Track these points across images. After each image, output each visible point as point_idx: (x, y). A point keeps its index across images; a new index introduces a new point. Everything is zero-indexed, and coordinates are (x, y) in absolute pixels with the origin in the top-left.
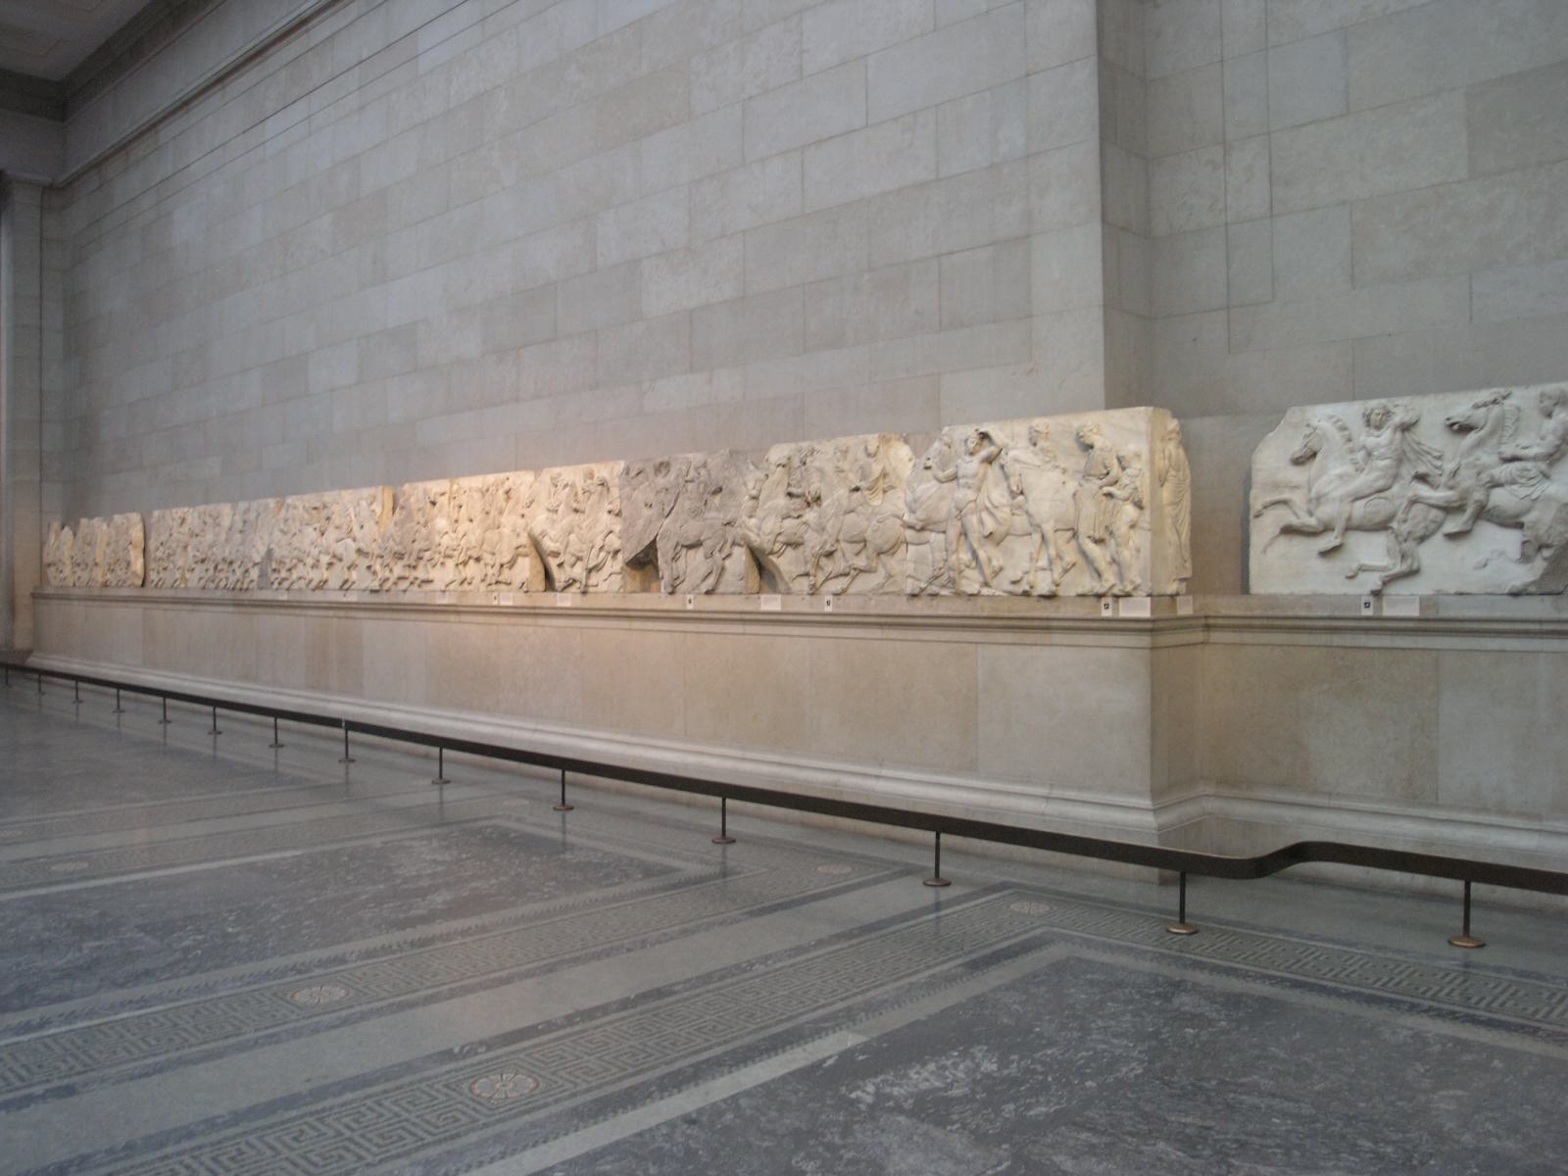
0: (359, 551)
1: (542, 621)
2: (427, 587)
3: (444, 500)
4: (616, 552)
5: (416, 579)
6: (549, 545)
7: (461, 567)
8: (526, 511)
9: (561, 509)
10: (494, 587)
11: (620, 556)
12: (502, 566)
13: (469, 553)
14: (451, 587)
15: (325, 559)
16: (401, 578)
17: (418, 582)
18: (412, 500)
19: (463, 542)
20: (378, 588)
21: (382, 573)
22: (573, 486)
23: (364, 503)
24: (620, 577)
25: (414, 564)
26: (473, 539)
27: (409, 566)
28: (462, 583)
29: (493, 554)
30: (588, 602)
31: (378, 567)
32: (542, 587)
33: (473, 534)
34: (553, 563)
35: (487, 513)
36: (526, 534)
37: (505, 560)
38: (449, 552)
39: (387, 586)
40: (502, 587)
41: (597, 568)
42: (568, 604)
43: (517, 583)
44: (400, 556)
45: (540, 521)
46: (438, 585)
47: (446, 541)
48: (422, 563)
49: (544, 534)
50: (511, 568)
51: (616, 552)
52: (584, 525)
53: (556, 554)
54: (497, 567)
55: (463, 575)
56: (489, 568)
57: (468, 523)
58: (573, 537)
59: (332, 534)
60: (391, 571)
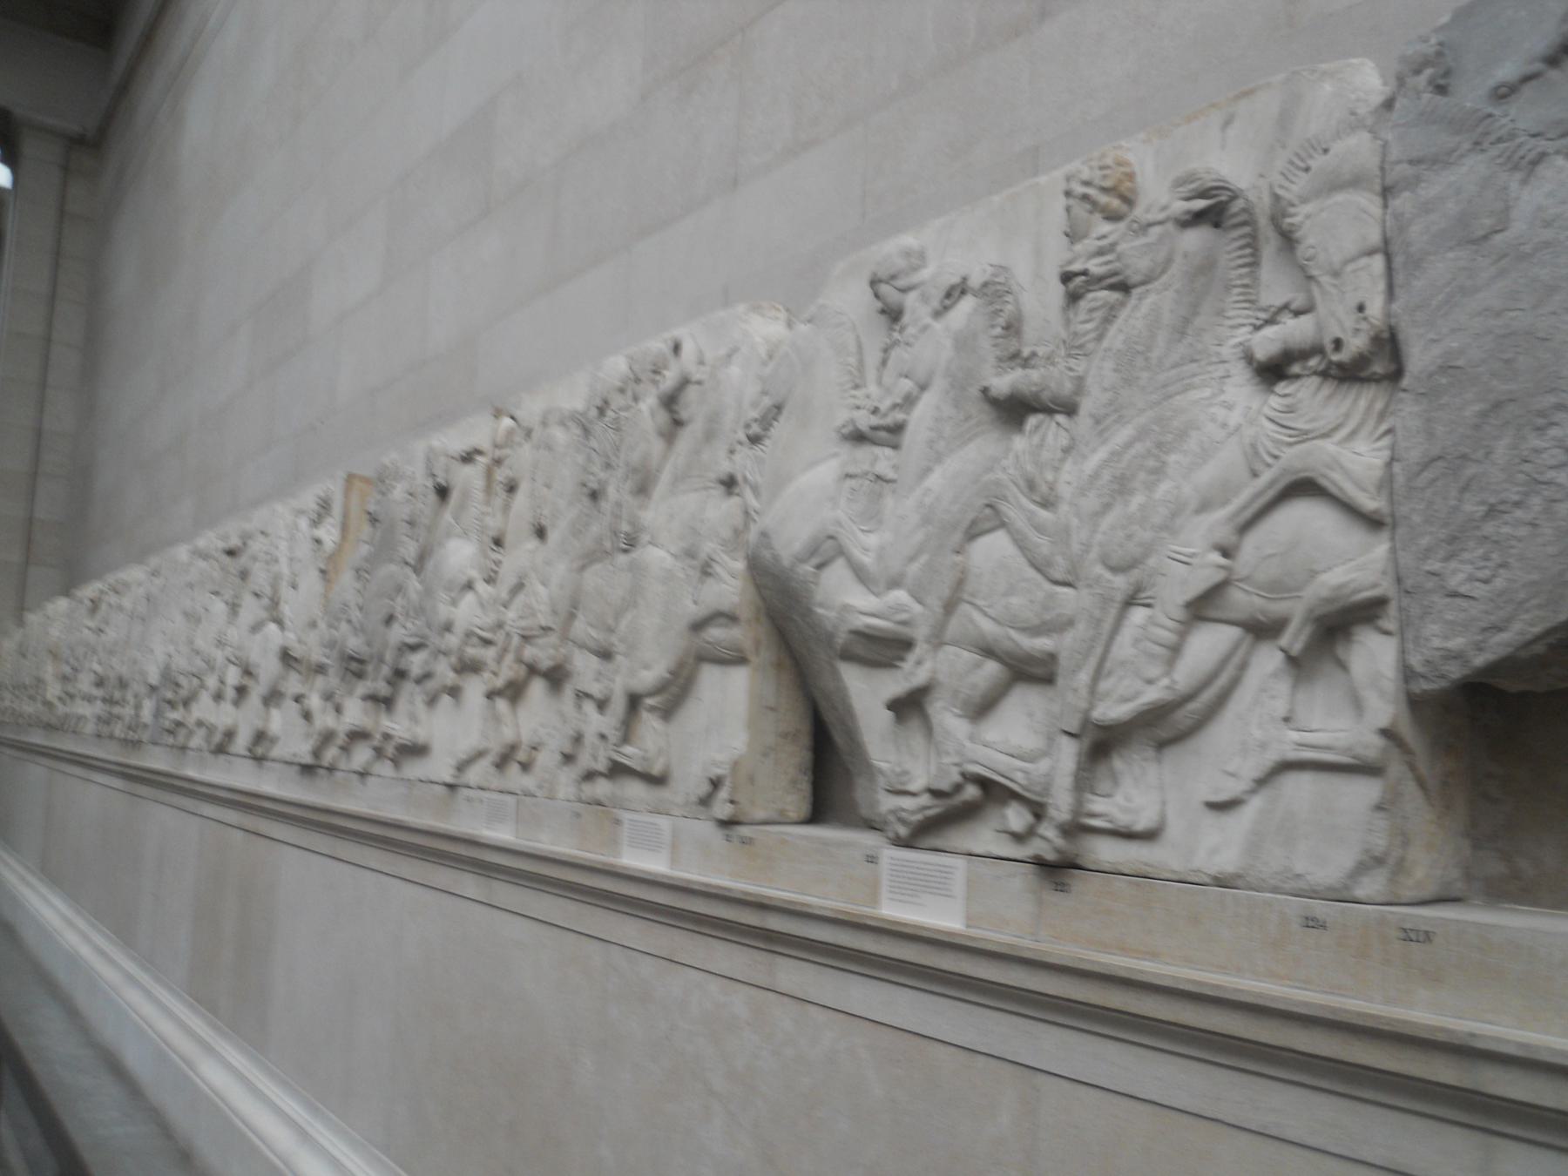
0: (286, 657)
1: (792, 974)
2: (415, 769)
3: (469, 478)
4: (1338, 625)
5: (387, 737)
6: (847, 601)
7: (502, 705)
8: (743, 463)
9: (920, 419)
10: (602, 788)
11: (1374, 656)
12: (634, 702)
13: (529, 652)
14: (474, 775)
15: (233, 676)
16: (358, 735)
17: (390, 750)
18: (398, 492)
19: (510, 615)
20: (308, 760)
21: (325, 720)
22: (994, 292)
23: (303, 523)
24: (1365, 791)
25: (383, 689)
26: (541, 599)
27: (373, 698)
28: (502, 762)
29: (605, 655)
30: (1074, 931)
31: (315, 702)
32: (797, 803)
33: (545, 575)
34: (866, 694)
35: (594, 496)
36: (740, 565)
37: (648, 677)
38: (473, 652)
39: (331, 754)
40: (634, 790)
41: (1163, 727)
42: (945, 918)
43: (688, 782)
44: (354, 667)
45: (807, 493)
46: (439, 767)
47: (467, 612)
48: (408, 687)
49: (827, 550)
50: (667, 713)
51: (1338, 625)
52: (1068, 478)
53: (883, 649)
54: (618, 706)
55: (508, 734)
56: (589, 708)
57: (532, 543)
58: (994, 548)
59: (251, 610)
60: (338, 710)
